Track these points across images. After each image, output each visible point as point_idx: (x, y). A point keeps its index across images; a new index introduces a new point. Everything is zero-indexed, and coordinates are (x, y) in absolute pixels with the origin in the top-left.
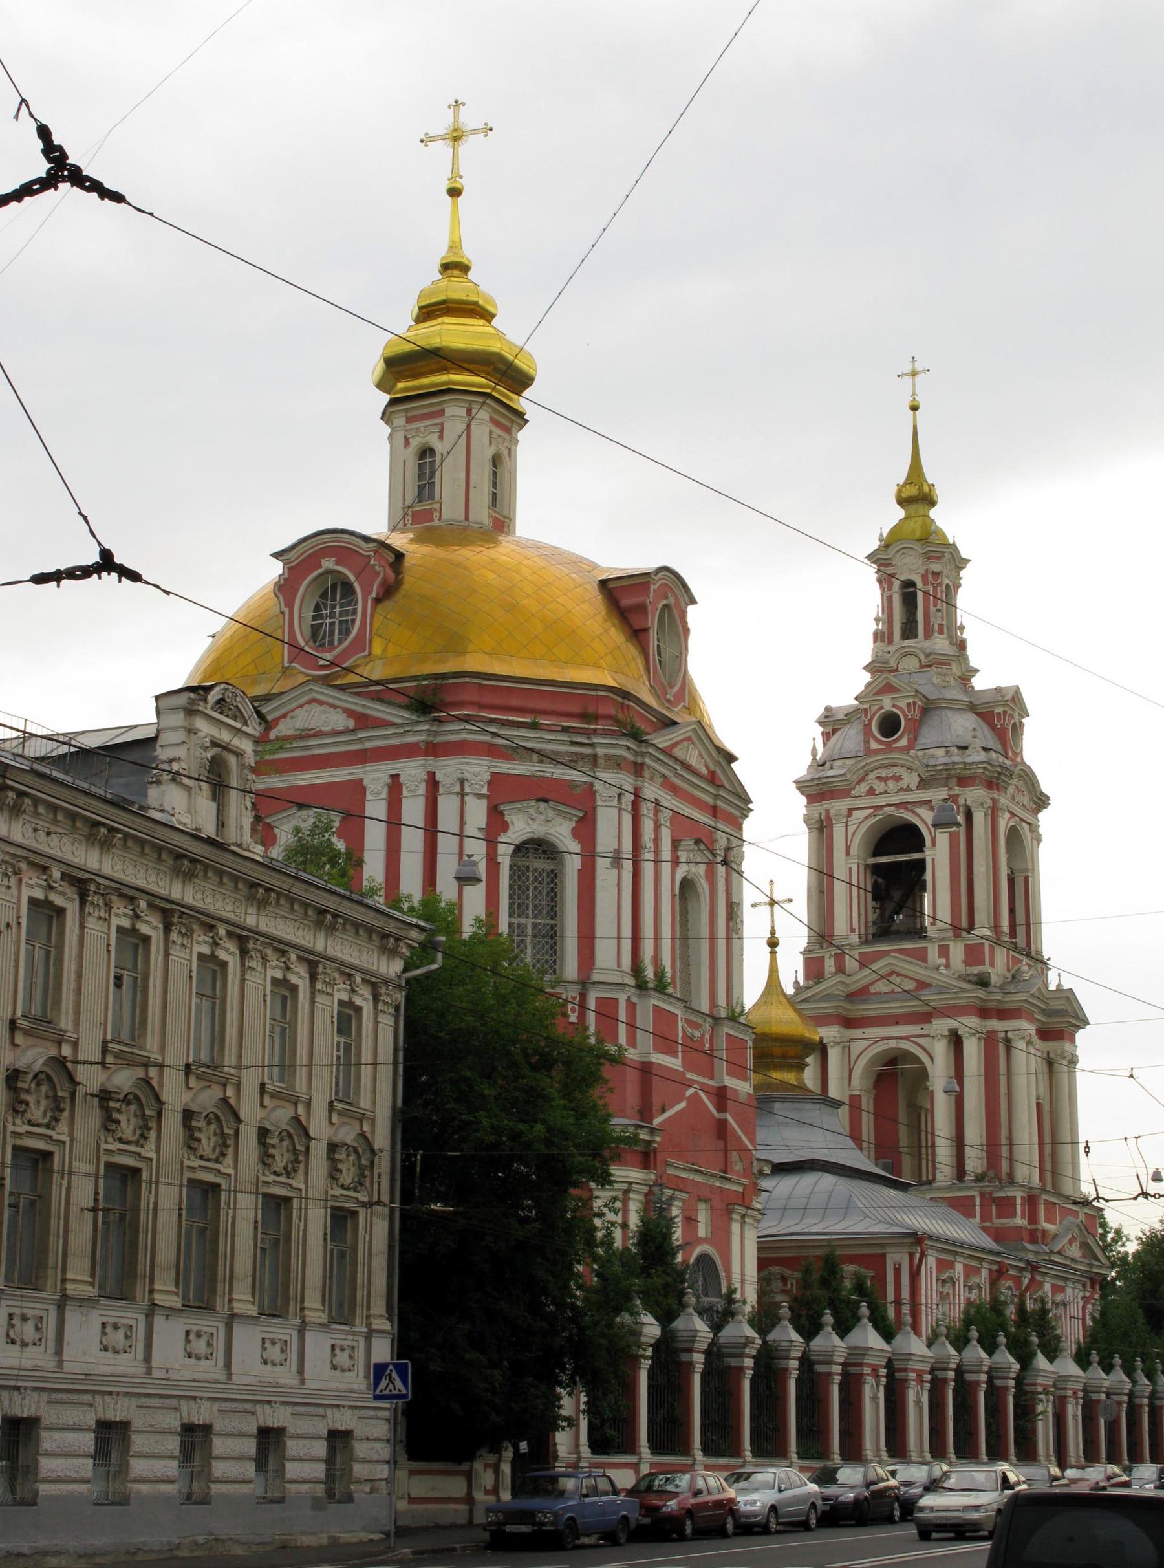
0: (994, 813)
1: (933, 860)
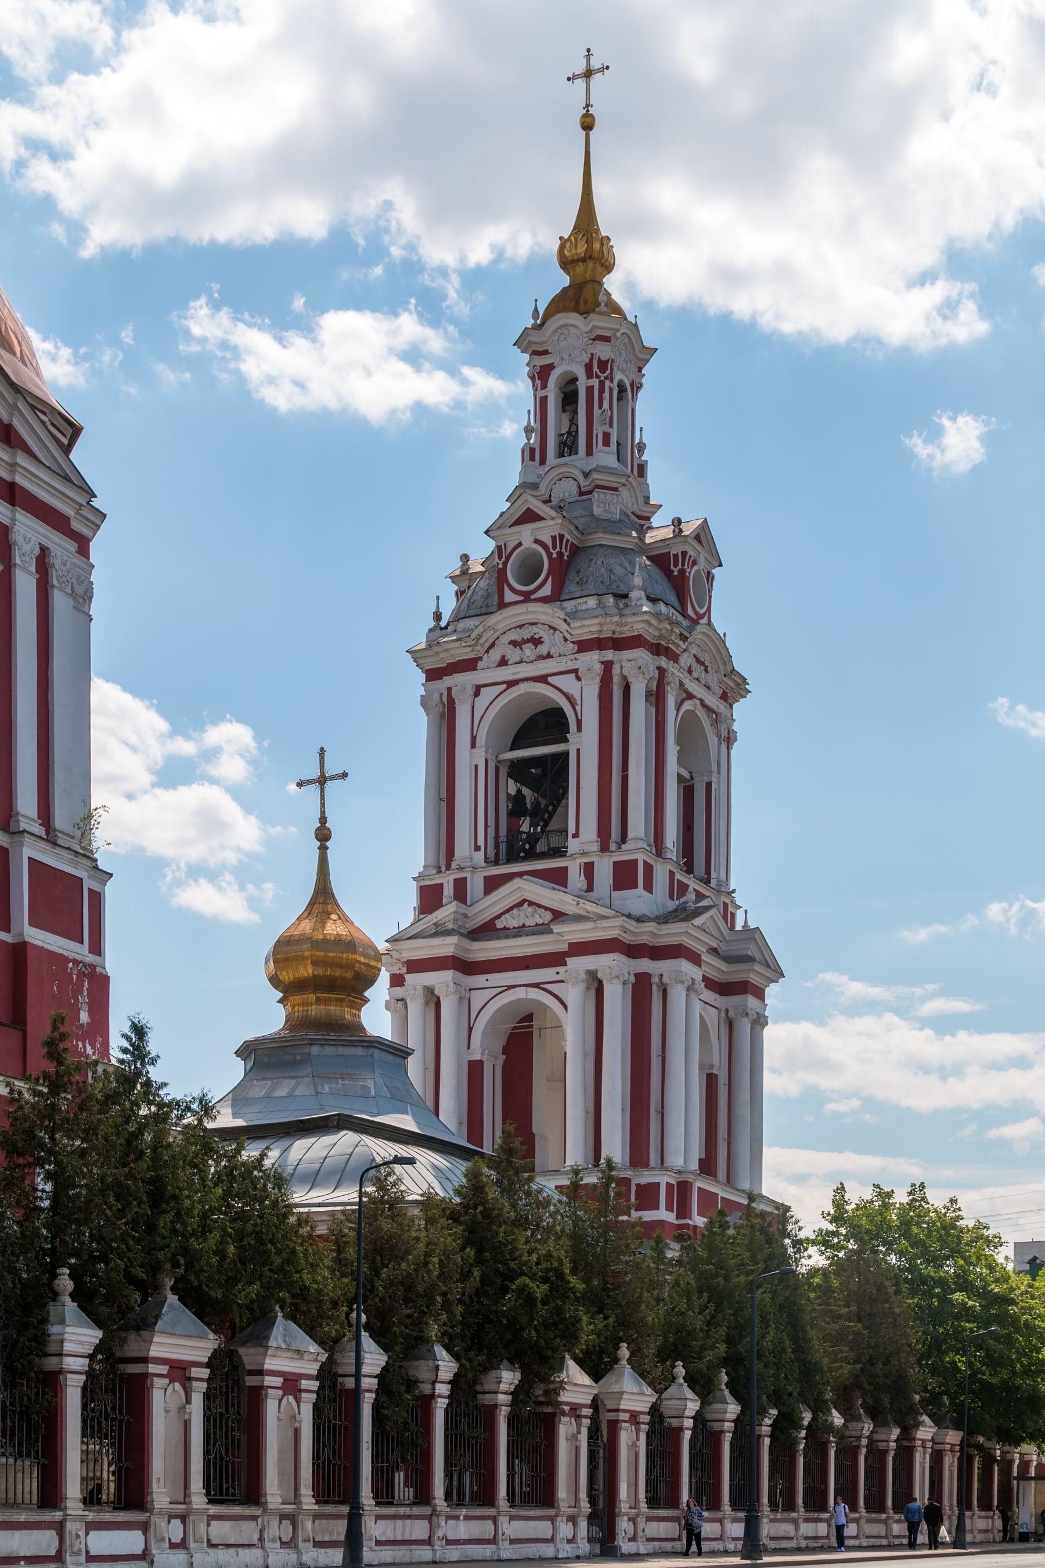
1: (578, 750)
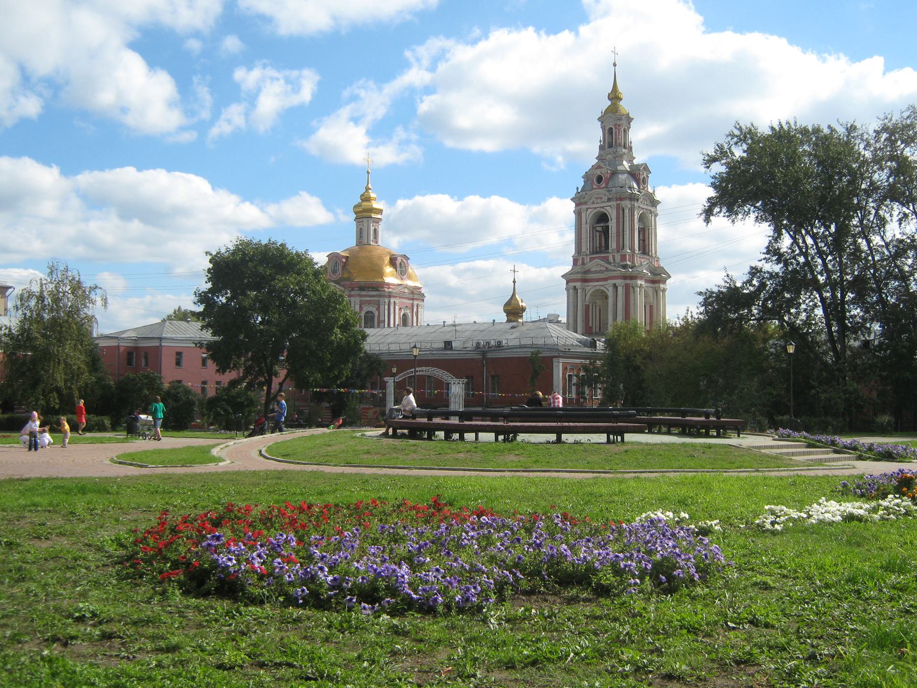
0: (632, 210)
